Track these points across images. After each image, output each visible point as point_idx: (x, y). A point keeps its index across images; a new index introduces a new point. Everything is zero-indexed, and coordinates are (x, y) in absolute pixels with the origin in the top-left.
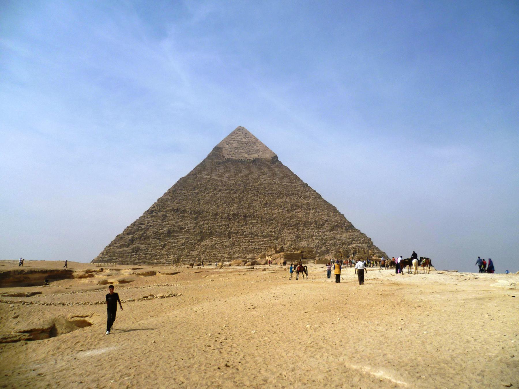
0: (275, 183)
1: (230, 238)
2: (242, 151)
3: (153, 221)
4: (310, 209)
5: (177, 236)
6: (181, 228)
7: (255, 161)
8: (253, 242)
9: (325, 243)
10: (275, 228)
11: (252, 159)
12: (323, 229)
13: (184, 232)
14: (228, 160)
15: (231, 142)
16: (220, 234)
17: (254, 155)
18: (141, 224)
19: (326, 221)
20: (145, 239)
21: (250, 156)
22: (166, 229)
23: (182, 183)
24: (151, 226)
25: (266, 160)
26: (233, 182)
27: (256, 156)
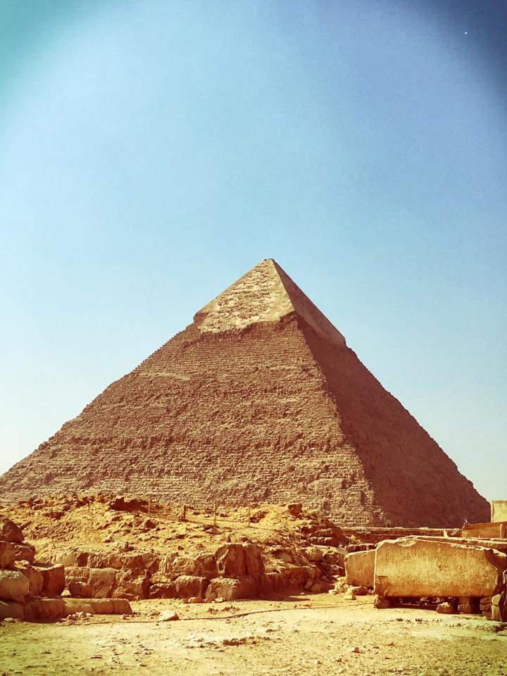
0: (257, 369)
1: (127, 480)
2: (236, 313)
3: (40, 461)
4: (285, 415)
5: (59, 482)
6: (68, 470)
7: (250, 329)
8: (157, 485)
9: (272, 480)
10: (203, 458)
11: (243, 327)
12: (284, 454)
13: (70, 474)
14: (206, 337)
15: (230, 297)
16: (117, 475)
17: (252, 318)
18: (23, 467)
19: (300, 436)
20: (14, 490)
21: (245, 320)
22: (48, 472)
23: (114, 386)
24: (31, 469)
25: (270, 324)
26: (189, 379)
27: (255, 319)
